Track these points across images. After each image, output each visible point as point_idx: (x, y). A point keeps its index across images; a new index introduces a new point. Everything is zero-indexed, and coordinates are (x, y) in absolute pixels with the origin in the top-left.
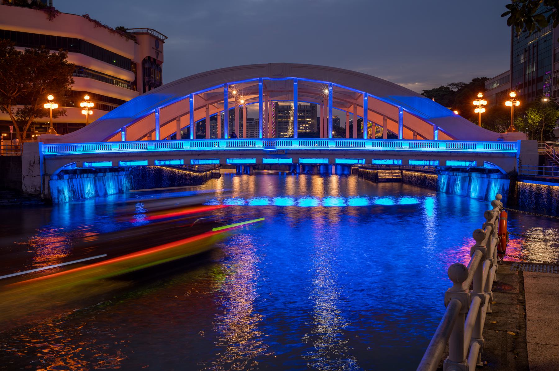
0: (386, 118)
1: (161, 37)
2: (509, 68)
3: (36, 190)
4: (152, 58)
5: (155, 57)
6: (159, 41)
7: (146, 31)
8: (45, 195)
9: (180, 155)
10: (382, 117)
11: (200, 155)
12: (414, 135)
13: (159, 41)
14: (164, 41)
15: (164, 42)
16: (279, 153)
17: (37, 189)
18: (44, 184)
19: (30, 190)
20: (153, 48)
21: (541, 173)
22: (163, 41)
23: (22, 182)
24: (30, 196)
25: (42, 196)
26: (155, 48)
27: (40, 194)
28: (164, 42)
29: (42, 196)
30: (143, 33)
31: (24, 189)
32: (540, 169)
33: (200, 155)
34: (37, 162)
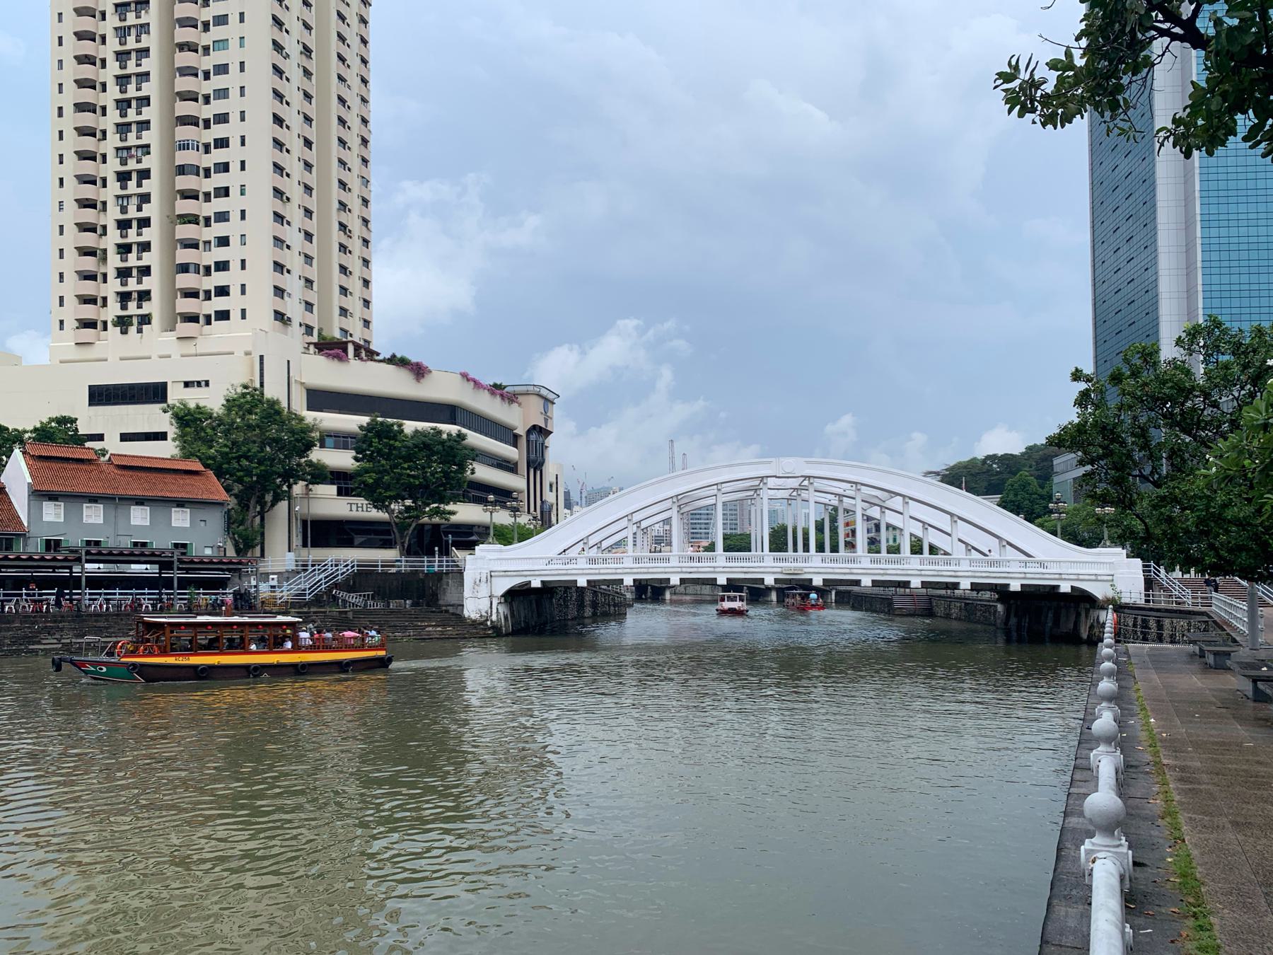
0: (926, 526)
3: (481, 616)
8: (492, 621)
10: (921, 524)
17: (484, 614)
18: (491, 608)
19: (474, 616)
21: (1147, 601)
23: (463, 605)
24: (474, 623)
25: (489, 623)
27: (487, 620)
29: (489, 623)
30: (527, 394)
31: (466, 614)
32: (1146, 595)
34: (484, 579)
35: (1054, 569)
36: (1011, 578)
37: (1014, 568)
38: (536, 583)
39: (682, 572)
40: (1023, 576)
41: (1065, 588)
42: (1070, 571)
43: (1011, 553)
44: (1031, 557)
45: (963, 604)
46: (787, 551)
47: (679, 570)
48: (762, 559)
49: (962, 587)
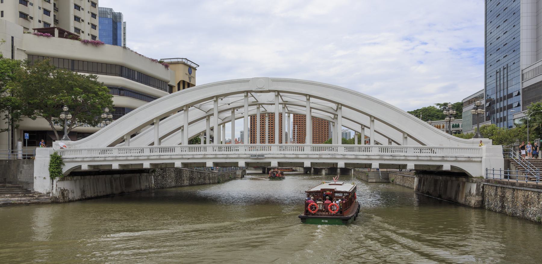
1: (194, 66)
2: (483, 87)
4: (186, 82)
5: (189, 82)
6: (192, 69)
7: (180, 60)
9: (172, 159)
11: (189, 159)
12: (389, 140)
13: (192, 69)
14: (196, 68)
15: (196, 70)
16: (259, 157)
20: (187, 74)
22: (195, 69)
26: (188, 74)
28: (196, 70)
33: (189, 159)
35: (440, 153)
36: (408, 160)
37: (410, 153)
38: (85, 167)
39: (183, 159)
40: (415, 158)
41: (447, 167)
42: (451, 155)
43: (411, 143)
44: (382, 145)
45: (402, 176)
46: (200, 144)
47: (180, 157)
48: (205, 149)
49: (373, 167)
